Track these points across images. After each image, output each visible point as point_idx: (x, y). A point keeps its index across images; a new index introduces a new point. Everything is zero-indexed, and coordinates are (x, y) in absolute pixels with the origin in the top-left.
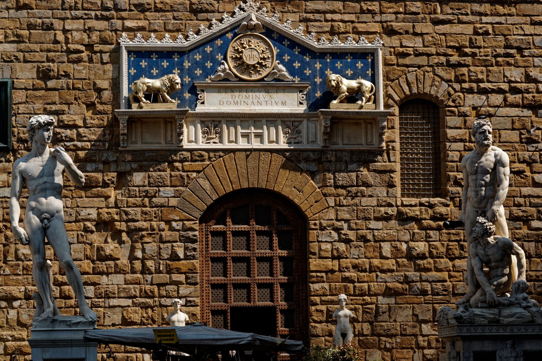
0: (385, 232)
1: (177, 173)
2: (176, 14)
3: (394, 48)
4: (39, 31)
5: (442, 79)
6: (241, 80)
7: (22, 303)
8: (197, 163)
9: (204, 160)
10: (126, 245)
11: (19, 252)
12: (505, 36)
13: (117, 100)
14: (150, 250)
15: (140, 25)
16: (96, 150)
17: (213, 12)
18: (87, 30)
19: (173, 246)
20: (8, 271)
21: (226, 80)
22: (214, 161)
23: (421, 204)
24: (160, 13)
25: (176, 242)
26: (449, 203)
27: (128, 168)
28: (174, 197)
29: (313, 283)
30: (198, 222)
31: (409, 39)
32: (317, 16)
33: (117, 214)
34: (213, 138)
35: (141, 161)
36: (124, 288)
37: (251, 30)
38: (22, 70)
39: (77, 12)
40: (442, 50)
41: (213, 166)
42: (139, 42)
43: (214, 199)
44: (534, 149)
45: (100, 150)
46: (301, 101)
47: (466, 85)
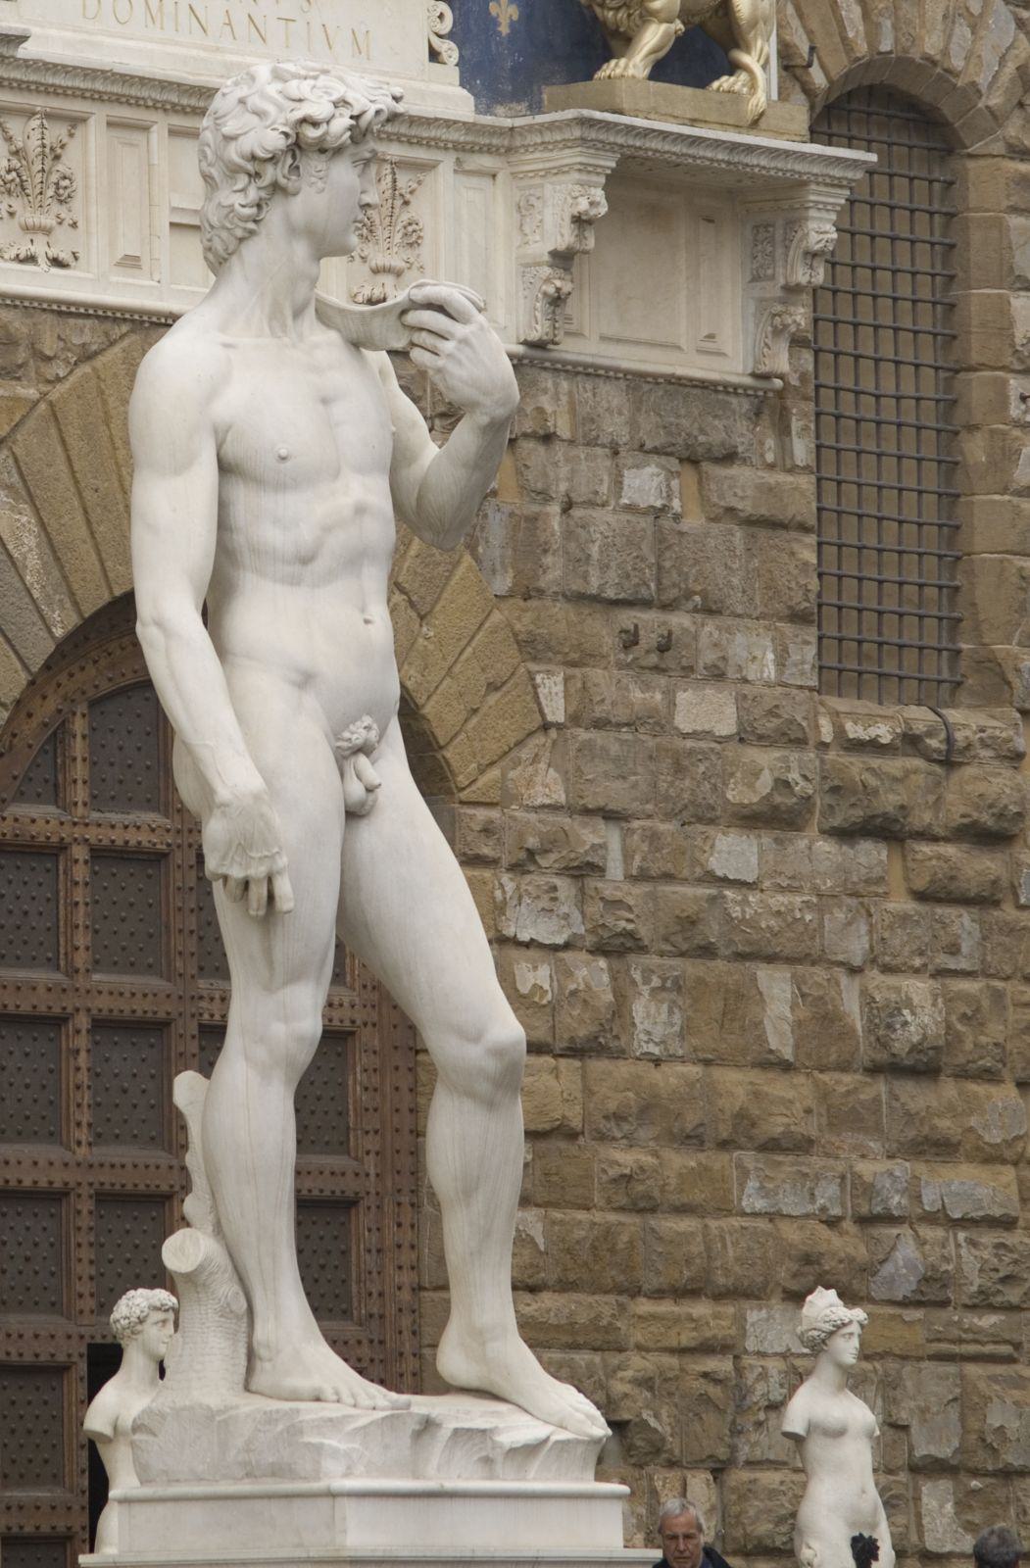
22: (59, 379)
23: (911, 742)
41: (51, 404)
46: (437, 43)
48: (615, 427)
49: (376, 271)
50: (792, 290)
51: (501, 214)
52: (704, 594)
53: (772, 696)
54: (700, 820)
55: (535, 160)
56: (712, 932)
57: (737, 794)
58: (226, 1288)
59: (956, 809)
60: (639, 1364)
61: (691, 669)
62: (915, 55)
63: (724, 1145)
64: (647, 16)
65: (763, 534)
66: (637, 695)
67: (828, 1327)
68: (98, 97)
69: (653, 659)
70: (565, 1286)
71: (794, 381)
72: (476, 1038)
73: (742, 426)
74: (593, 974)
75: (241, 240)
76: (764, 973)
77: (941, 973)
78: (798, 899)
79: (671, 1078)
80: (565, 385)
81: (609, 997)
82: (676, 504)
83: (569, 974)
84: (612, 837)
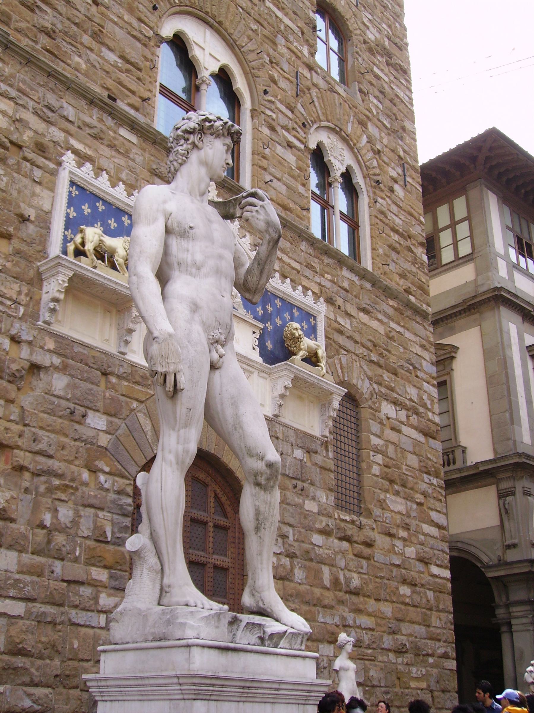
1: (113, 393)
2: (131, 163)
5: (366, 374)
10: (29, 496)
12: (405, 348)
13: (44, 246)
14: (64, 515)
15: (89, 152)
16: (3, 313)
18: (17, 120)
19: (97, 516)
24: (114, 153)
25: (102, 509)
26: (374, 526)
27: (47, 363)
28: (106, 432)
31: (343, 317)
33: (20, 436)
35: (66, 356)
36: (16, 580)
39: (9, 89)
40: (364, 341)
42: (86, 172)
44: (428, 481)
45: (9, 316)
47: (383, 390)
48: (292, 439)
50: (330, 417)
52: (311, 480)
54: (310, 530)
56: (313, 556)
58: (152, 560)
59: (361, 539)
61: (308, 496)
64: (300, 349)
65: (323, 471)
66: (296, 499)
67: (345, 642)
69: (300, 492)
72: (262, 459)
73: (319, 446)
74: (286, 561)
75: (181, 165)
77: (360, 573)
78: (331, 552)
79: (303, 588)
80: (281, 428)
82: (305, 459)
83: (280, 560)
84: (291, 530)
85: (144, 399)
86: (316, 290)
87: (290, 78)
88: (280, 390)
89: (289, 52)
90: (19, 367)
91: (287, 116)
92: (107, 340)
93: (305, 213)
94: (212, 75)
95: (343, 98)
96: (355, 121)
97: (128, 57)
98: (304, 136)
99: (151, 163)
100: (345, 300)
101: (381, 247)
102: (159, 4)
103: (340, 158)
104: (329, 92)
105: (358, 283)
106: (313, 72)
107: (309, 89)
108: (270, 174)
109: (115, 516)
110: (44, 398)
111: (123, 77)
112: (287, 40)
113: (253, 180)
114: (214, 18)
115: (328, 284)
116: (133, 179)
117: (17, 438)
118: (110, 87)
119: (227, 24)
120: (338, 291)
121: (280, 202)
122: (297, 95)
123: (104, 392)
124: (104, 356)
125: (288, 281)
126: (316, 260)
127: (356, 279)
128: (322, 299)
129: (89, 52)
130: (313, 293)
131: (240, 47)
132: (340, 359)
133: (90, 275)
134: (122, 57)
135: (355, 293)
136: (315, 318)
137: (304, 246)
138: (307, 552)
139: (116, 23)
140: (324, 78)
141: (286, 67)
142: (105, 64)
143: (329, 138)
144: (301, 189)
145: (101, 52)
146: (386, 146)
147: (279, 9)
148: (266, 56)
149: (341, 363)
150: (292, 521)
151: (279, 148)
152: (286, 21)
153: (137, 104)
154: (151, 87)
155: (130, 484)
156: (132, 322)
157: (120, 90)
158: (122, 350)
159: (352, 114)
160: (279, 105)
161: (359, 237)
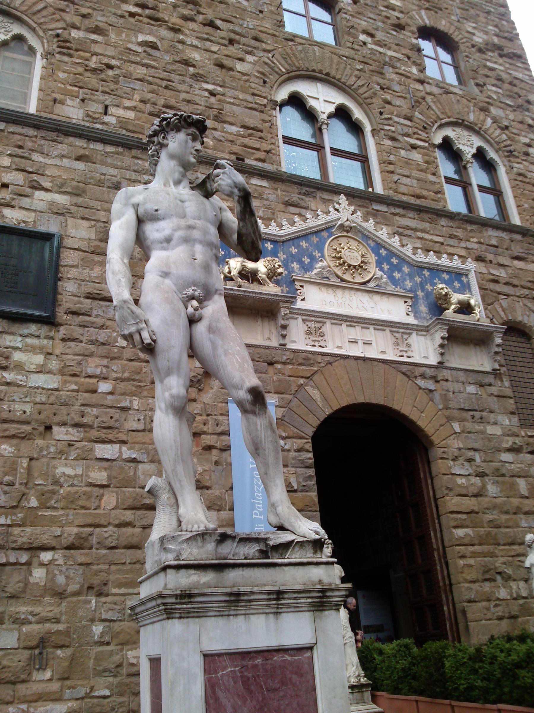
0: (519, 465)
1: (281, 377)
2: (266, 202)
3: (483, 273)
4: (101, 188)
6: (343, 280)
7: (56, 557)
8: (303, 367)
9: (311, 365)
10: (220, 467)
11: (57, 471)
17: (306, 208)
20: (34, 502)
21: (327, 278)
29: (456, 527)
30: (310, 441)
31: (496, 269)
32: (409, 232)
33: (205, 424)
34: (319, 341)
37: (348, 232)
38: (76, 227)
43: (327, 413)
49: (401, 351)
50: (496, 353)
51: (429, 342)
53: (509, 428)
55: (433, 331)
57: (505, 445)
60: (502, 560)
62: (517, 320)
63: (515, 513)
64: (452, 304)
68: (328, 318)
70: (480, 544)
71: (502, 372)
74: (477, 481)
76: (518, 480)
81: (481, 484)
82: (480, 393)
83: (470, 480)
85: (309, 375)
86: (463, 253)
87: (403, 95)
88: (439, 341)
89: (398, 76)
90: (194, 374)
91: (406, 125)
92: (268, 338)
93: (439, 196)
94: (330, 117)
95: (459, 95)
96: (476, 109)
97: (248, 125)
98: (426, 136)
99: (283, 197)
100: (495, 254)
101: (525, 202)
102: (268, 78)
103: (469, 143)
104: (444, 95)
105: (506, 237)
106: (425, 85)
107: (424, 98)
108: (399, 174)
109: (299, 469)
110: (221, 392)
111: (247, 141)
112: (393, 67)
113: (383, 184)
114: (321, 72)
115: (476, 246)
116: (270, 213)
117: (202, 426)
118: (236, 151)
119: (333, 73)
120: (486, 249)
121: (413, 194)
122: (413, 107)
123: (272, 377)
124: (267, 351)
125: (432, 253)
126: (459, 230)
127: (504, 235)
128: (469, 260)
129: (213, 131)
130: (460, 256)
131: (350, 87)
132: (501, 304)
133: (237, 293)
134: (243, 127)
135: (505, 247)
136: (467, 275)
137: (443, 222)
138: (498, 470)
139: (233, 104)
140: (437, 86)
141: (397, 88)
142: (229, 136)
143: (454, 131)
144: (432, 178)
145: (224, 128)
146: (513, 121)
147: (381, 46)
148: (376, 86)
149: (502, 307)
150: (476, 446)
151: (403, 152)
152: (390, 53)
153: (262, 157)
154: (273, 141)
155: (308, 442)
156: (283, 319)
157: (245, 151)
158: (282, 342)
159: (471, 104)
160: (396, 119)
161: (504, 201)
